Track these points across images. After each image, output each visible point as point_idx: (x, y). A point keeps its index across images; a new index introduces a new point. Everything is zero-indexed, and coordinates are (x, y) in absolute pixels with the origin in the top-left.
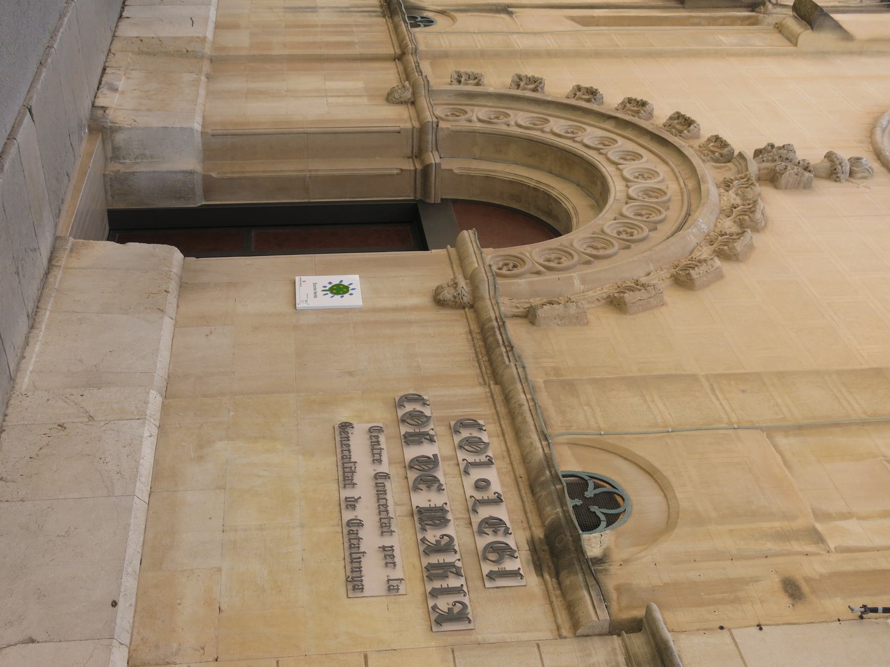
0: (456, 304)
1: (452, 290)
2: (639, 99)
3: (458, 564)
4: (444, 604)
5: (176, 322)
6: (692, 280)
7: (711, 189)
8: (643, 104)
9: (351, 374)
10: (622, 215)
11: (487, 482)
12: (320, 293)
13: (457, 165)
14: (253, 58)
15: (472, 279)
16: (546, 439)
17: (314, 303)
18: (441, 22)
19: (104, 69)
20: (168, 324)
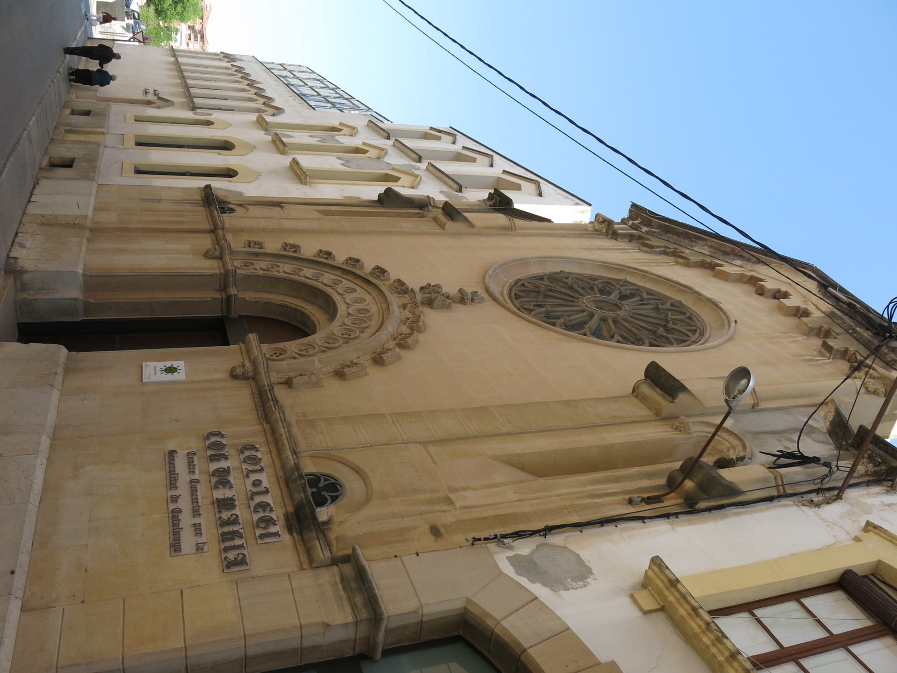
0: (244, 377)
1: (242, 369)
3: (241, 531)
4: (231, 555)
6: (383, 360)
8: (358, 261)
9: (177, 421)
10: (345, 324)
11: (260, 481)
12: (158, 373)
13: (248, 296)
14: (118, 229)
15: (254, 362)
16: (296, 454)
17: (154, 379)
18: (239, 211)
19: (17, 234)
20: (56, 393)
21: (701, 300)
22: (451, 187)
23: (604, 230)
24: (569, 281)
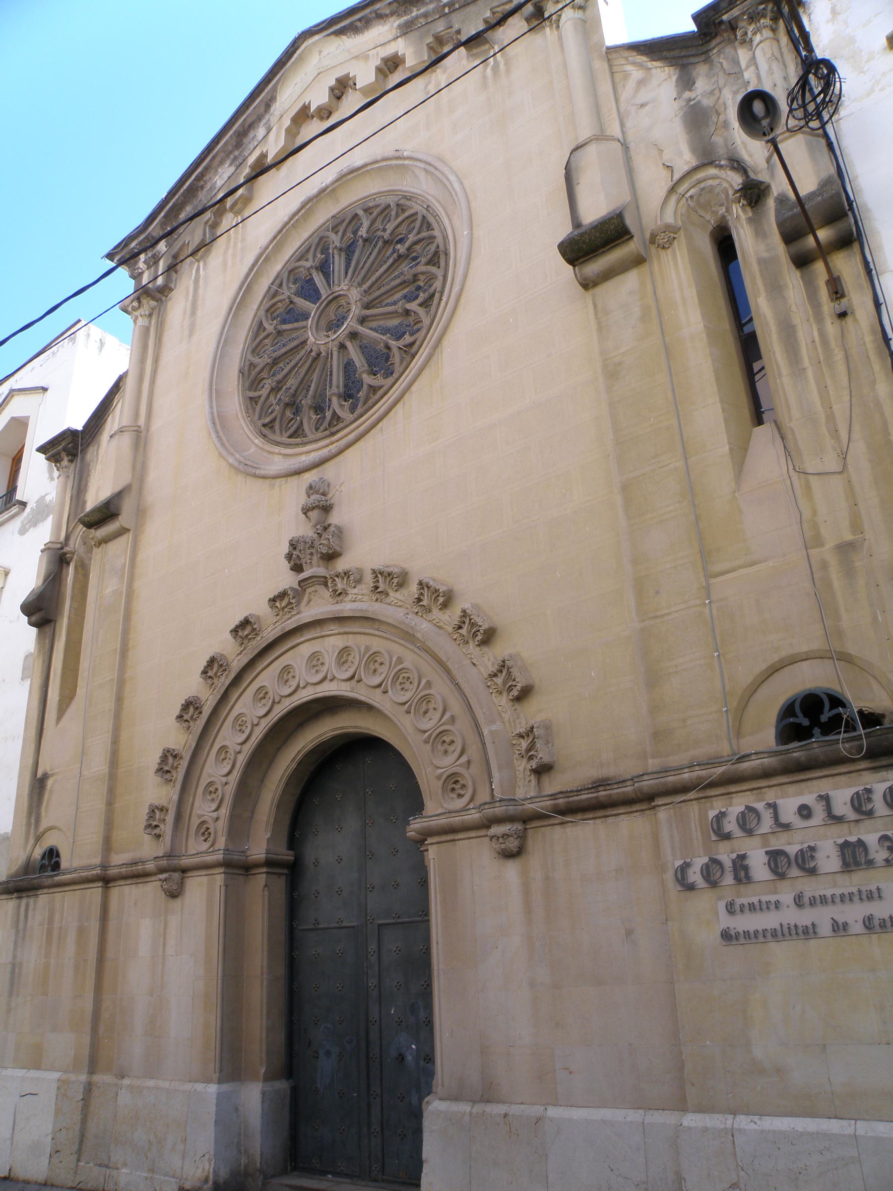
2: (205, 664)
5: (548, 1104)
7: (347, 607)
9: (629, 933)
21: (334, 190)
22: (13, 517)
23: (153, 303)
24: (261, 362)
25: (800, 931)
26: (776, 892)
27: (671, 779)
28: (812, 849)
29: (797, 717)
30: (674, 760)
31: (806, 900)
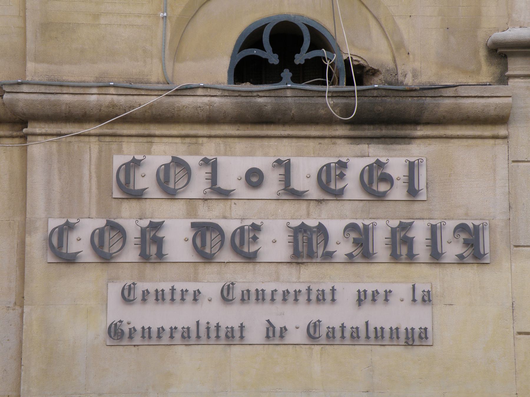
4: (452, 249)
25: (222, 334)
26: (196, 280)
27: (67, 98)
28: (256, 228)
29: (263, 49)
30: (71, 73)
31: (237, 293)
